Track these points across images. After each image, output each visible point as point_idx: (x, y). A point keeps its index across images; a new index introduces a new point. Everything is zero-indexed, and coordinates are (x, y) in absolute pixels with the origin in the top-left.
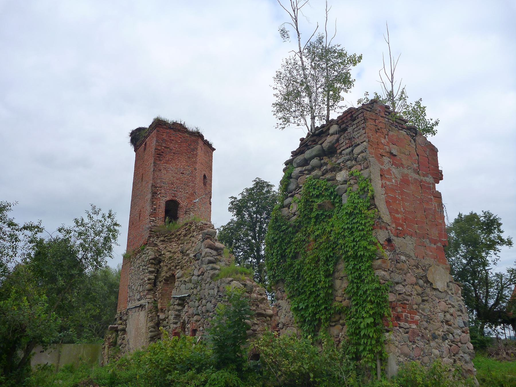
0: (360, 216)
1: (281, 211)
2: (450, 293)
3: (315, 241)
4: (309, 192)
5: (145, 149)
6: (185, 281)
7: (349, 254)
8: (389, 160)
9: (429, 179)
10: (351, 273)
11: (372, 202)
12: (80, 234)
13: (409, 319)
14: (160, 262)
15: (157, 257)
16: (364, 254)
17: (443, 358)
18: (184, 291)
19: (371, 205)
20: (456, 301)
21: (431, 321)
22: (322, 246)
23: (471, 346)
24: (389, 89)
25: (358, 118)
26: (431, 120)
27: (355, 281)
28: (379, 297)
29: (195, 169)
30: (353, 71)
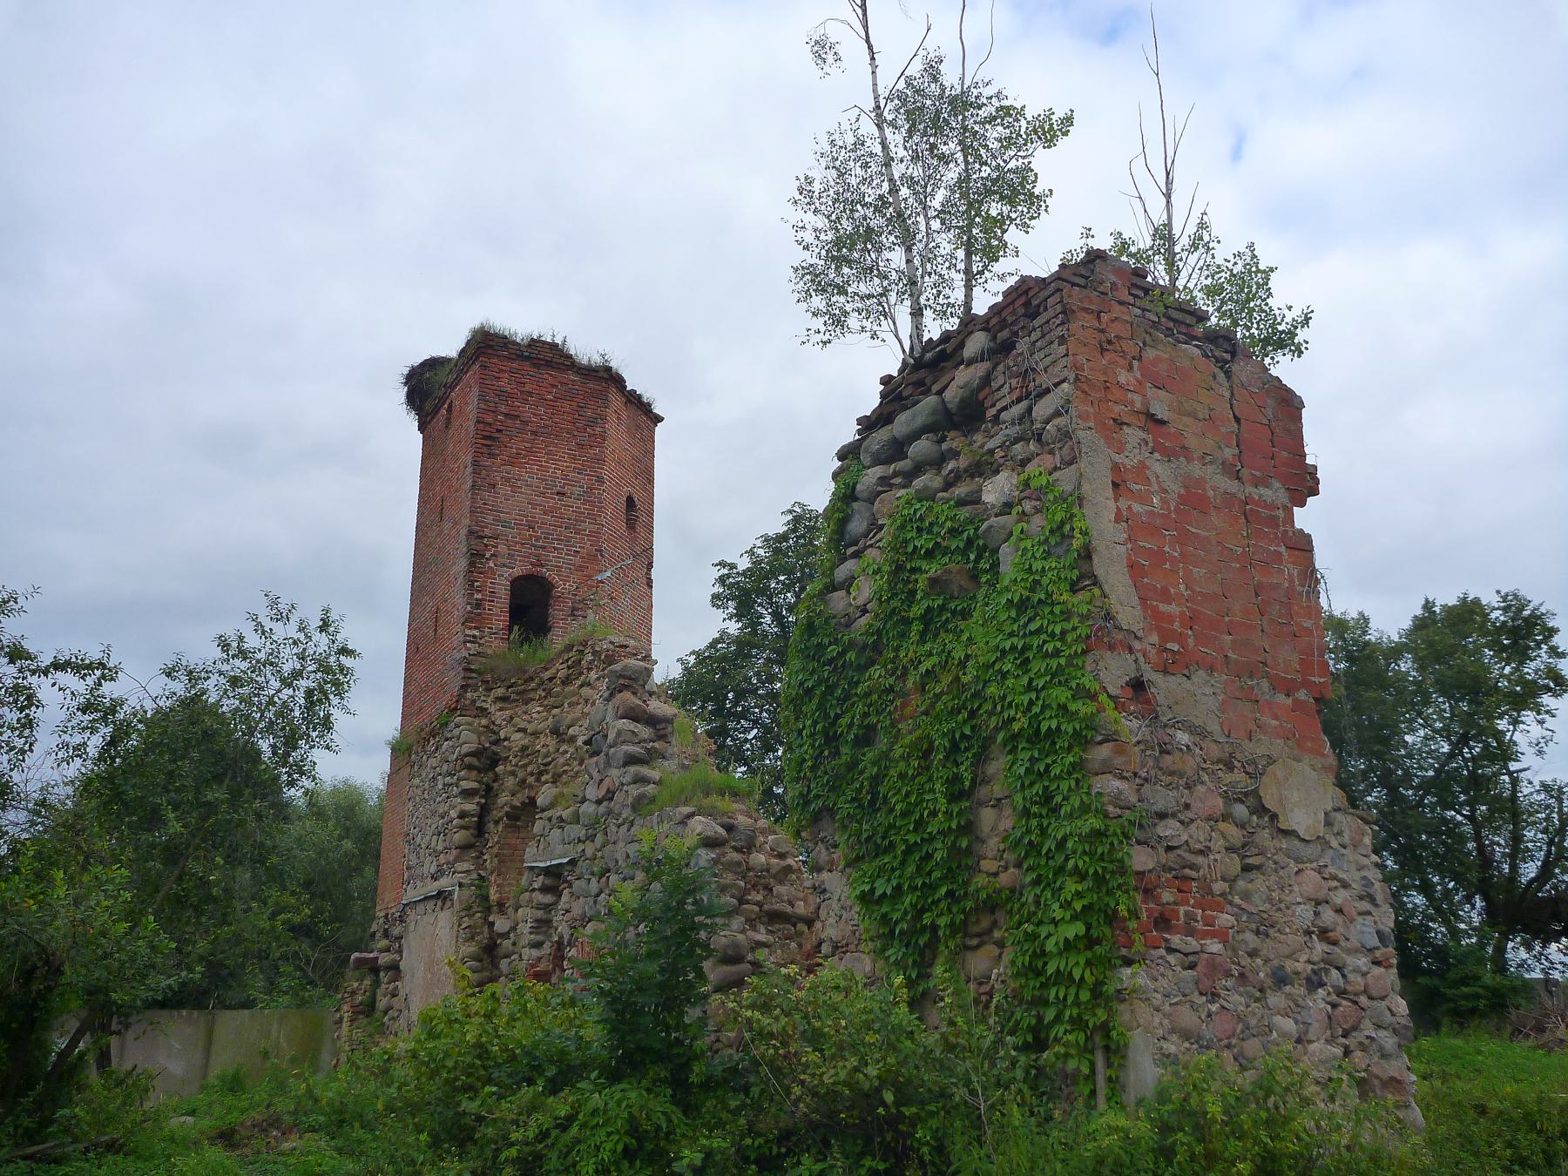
0: (1047, 610)
1: (826, 603)
2: (1334, 844)
3: (922, 689)
4: (906, 542)
5: (448, 422)
6: (561, 819)
7: (1016, 727)
8: (1142, 435)
9: (1275, 493)
10: (1023, 785)
11: (1085, 567)
12: (235, 681)
13: (1200, 926)
14: (495, 761)
15: (485, 749)
16: (1058, 728)
17: (1310, 1042)
18: (559, 848)
19: (1081, 577)
20: (1353, 867)
21: (1271, 931)
22: (939, 706)
23: (1402, 1006)
24: (1159, 217)
25: (1046, 309)
26: (1290, 308)
27: (1035, 809)
28: (1102, 858)
29: (601, 481)
30: (1047, 165)
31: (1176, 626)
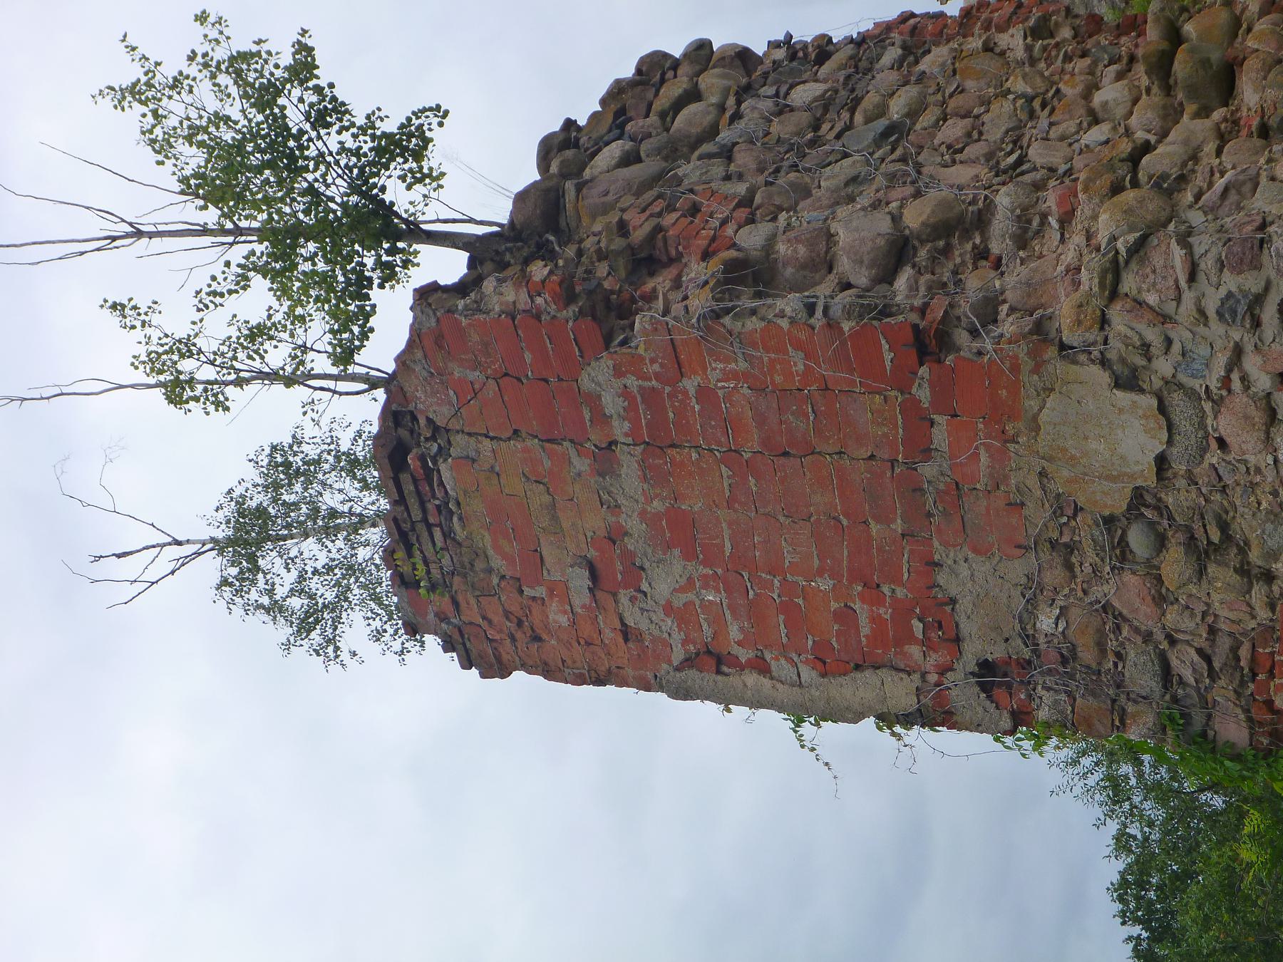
2: (1164, 366)
31: (886, 613)
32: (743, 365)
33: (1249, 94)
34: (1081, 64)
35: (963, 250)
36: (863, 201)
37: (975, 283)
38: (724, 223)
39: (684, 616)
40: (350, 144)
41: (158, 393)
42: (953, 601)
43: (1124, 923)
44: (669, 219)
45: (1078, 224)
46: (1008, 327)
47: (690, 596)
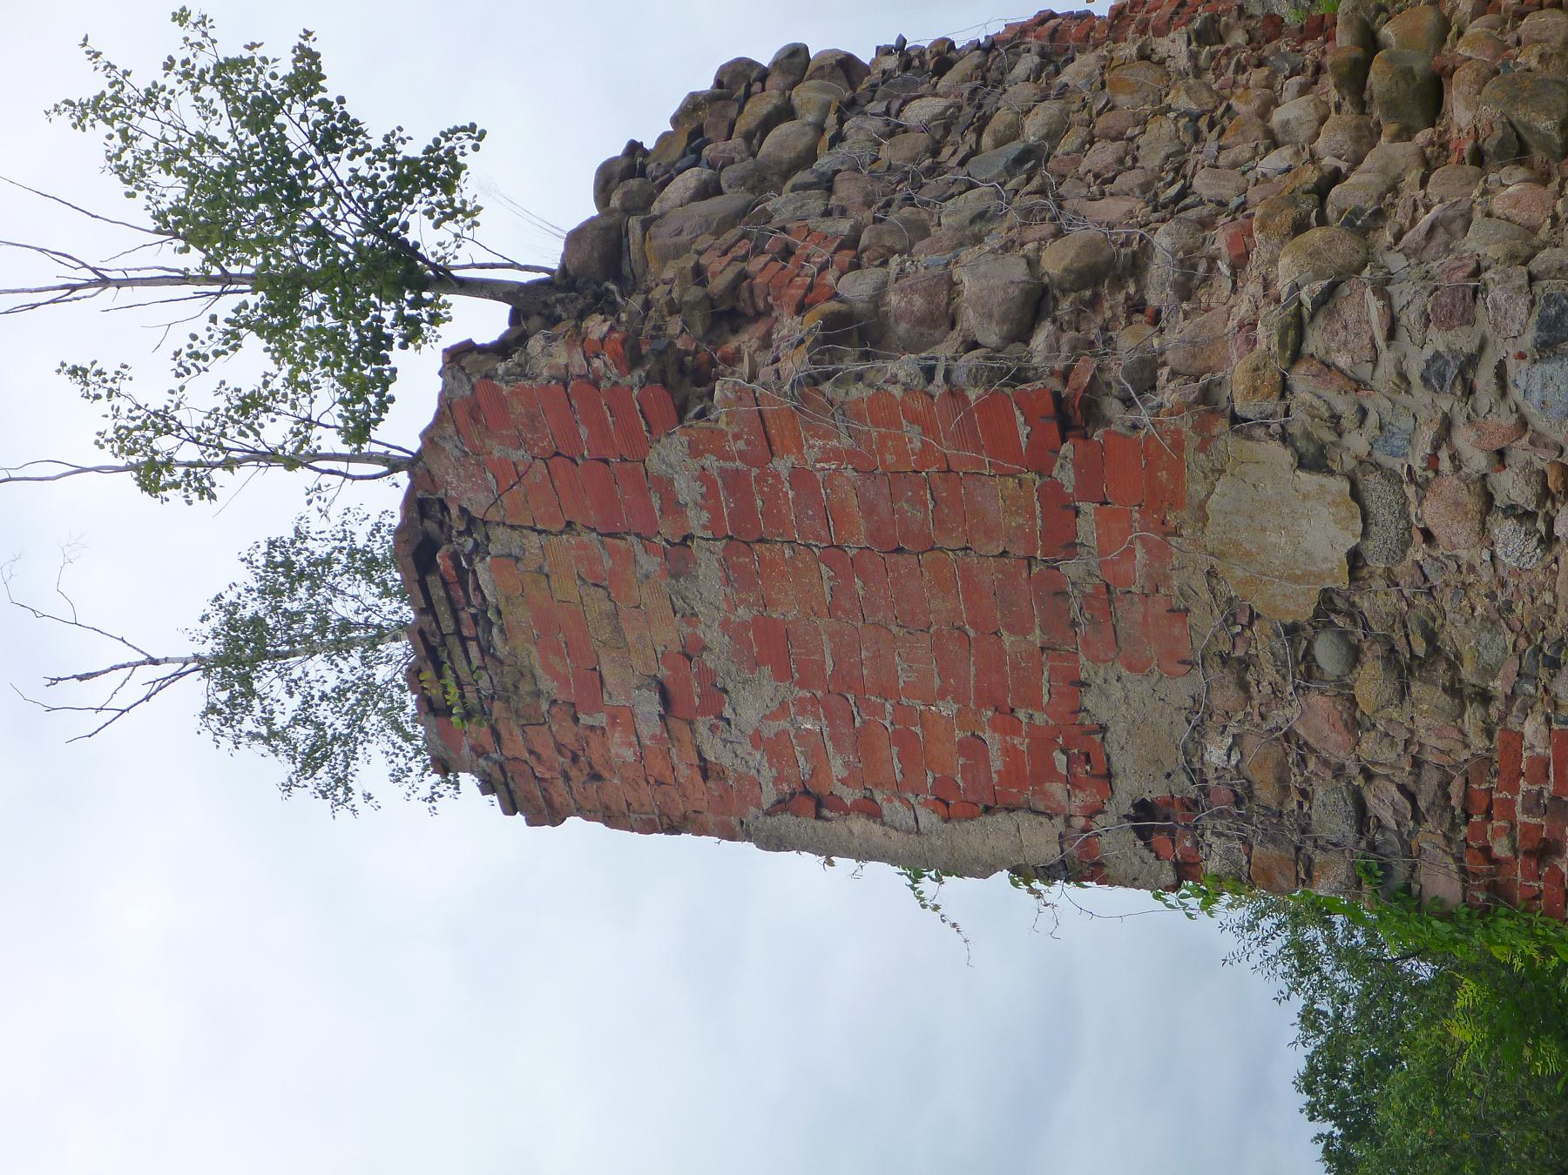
2: (1357, 442)
31: (1021, 743)
32: (847, 442)
33: (1461, 112)
34: (1257, 76)
35: (1113, 302)
36: (992, 242)
37: (1129, 341)
38: (823, 268)
39: (776, 749)
40: (365, 171)
41: (129, 478)
42: (1103, 729)
43: (1312, 1119)
44: (755, 264)
45: (1253, 270)
46: (1169, 394)
47: (784, 724)
